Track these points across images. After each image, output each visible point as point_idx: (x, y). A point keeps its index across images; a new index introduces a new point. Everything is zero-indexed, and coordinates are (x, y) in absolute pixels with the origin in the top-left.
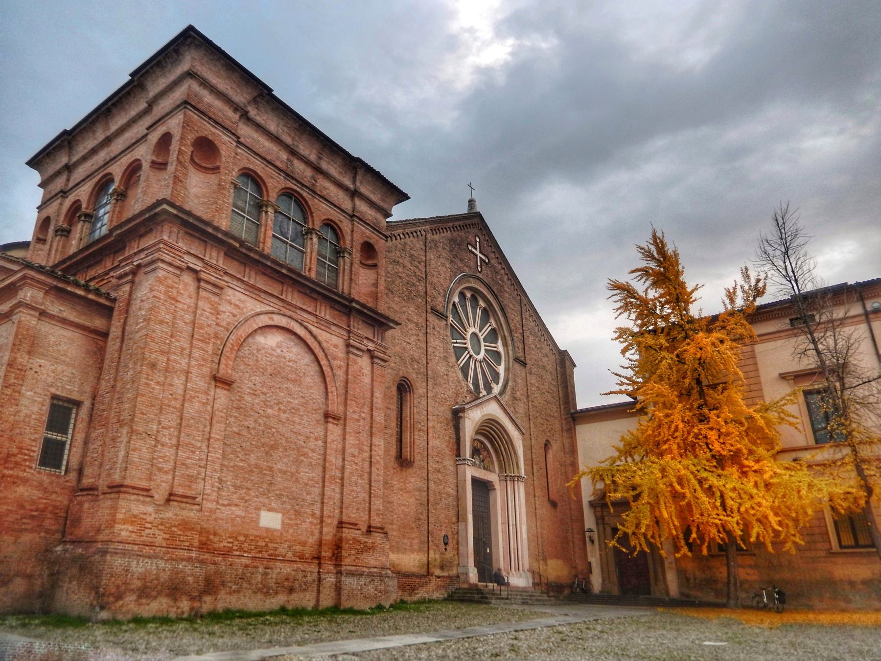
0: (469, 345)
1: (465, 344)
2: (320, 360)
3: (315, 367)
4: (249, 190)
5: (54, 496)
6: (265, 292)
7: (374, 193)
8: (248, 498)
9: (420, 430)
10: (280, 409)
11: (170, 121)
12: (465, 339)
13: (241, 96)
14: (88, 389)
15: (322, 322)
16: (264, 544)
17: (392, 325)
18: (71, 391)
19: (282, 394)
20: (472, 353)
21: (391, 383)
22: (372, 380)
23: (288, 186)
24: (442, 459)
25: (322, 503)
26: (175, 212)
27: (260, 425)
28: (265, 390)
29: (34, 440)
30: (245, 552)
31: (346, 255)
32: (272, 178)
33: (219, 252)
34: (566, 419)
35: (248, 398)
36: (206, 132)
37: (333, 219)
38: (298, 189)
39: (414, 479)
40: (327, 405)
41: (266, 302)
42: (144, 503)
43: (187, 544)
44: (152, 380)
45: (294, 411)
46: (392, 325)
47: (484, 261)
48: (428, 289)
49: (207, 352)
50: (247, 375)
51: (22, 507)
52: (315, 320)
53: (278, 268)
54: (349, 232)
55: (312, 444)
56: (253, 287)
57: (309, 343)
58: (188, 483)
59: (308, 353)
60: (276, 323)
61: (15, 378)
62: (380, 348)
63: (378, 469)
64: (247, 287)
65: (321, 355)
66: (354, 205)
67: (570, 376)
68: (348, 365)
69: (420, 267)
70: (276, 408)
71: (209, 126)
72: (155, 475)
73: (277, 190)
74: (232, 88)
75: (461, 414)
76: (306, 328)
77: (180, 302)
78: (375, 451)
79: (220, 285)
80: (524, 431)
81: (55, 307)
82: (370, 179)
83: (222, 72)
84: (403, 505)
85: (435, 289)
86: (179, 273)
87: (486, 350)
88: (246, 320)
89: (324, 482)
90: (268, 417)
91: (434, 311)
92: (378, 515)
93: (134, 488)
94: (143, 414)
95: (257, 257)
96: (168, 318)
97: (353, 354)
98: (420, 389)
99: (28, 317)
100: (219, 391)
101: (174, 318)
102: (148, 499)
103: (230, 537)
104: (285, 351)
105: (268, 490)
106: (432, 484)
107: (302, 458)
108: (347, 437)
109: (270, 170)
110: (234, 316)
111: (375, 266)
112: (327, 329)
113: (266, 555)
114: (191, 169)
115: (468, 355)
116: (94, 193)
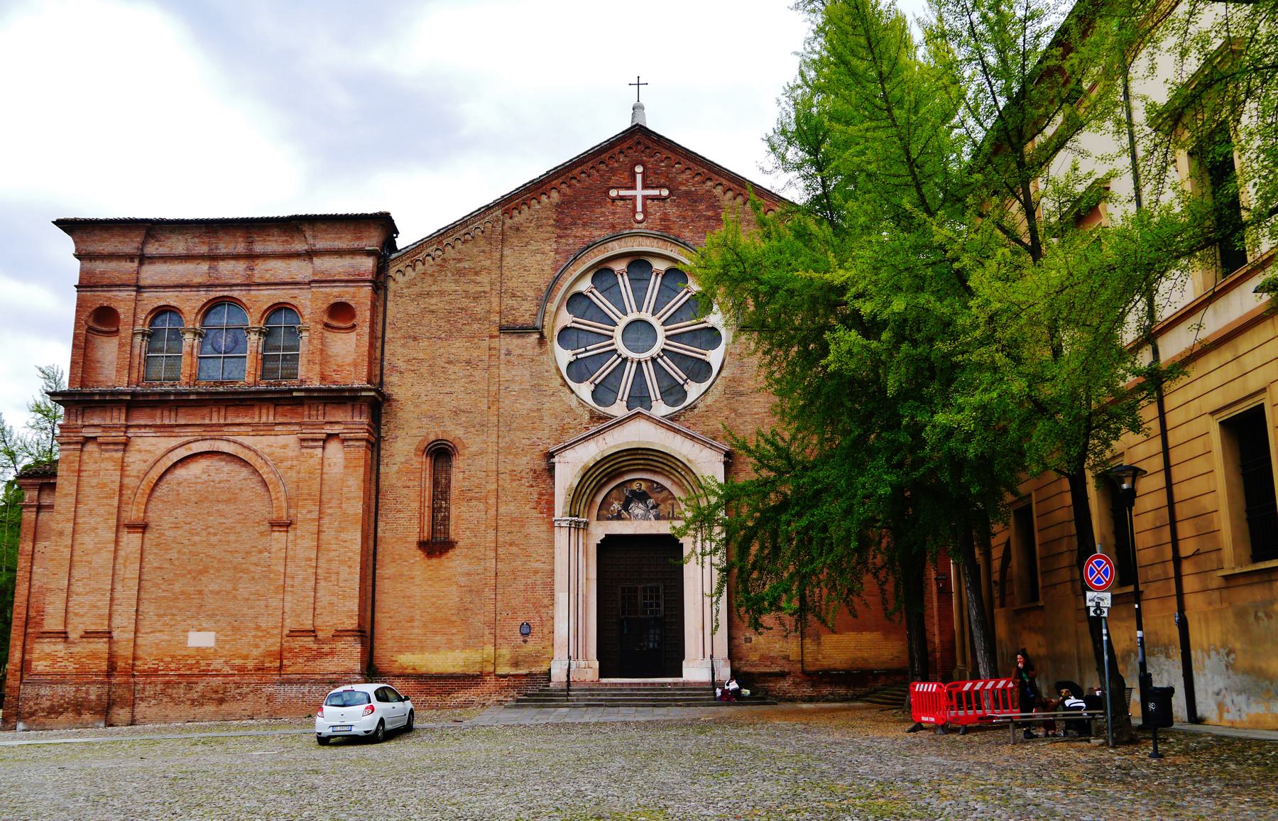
1: (613, 344)
3: (255, 478)
6: (177, 426)
7: (340, 238)
8: (173, 623)
13: (129, 245)
20: (625, 352)
24: (523, 526)
28: (189, 520)
32: (188, 300)
35: (170, 533)
37: (281, 300)
38: (226, 294)
39: (454, 563)
42: (55, 644)
47: (653, 198)
50: (166, 512)
52: (250, 429)
55: (254, 559)
56: (163, 426)
63: (350, 567)
65: (257, 463)
70: (204, 533)
75: (553, 460)
76: (235, 442)
82: (324, 227)
83: (105, 235)
84: (433, 597)
85: (514, 295)
86: (79, 447)
87: (667, 337)
90: (194, 544)
92: (351, 617)
97: (307, 447)
100: (130, 535)
105: (198, 614)
107: (241, 574)
109: (186, 293)
110: (145, 462)
113: (196, 671)
115: (620, 360)
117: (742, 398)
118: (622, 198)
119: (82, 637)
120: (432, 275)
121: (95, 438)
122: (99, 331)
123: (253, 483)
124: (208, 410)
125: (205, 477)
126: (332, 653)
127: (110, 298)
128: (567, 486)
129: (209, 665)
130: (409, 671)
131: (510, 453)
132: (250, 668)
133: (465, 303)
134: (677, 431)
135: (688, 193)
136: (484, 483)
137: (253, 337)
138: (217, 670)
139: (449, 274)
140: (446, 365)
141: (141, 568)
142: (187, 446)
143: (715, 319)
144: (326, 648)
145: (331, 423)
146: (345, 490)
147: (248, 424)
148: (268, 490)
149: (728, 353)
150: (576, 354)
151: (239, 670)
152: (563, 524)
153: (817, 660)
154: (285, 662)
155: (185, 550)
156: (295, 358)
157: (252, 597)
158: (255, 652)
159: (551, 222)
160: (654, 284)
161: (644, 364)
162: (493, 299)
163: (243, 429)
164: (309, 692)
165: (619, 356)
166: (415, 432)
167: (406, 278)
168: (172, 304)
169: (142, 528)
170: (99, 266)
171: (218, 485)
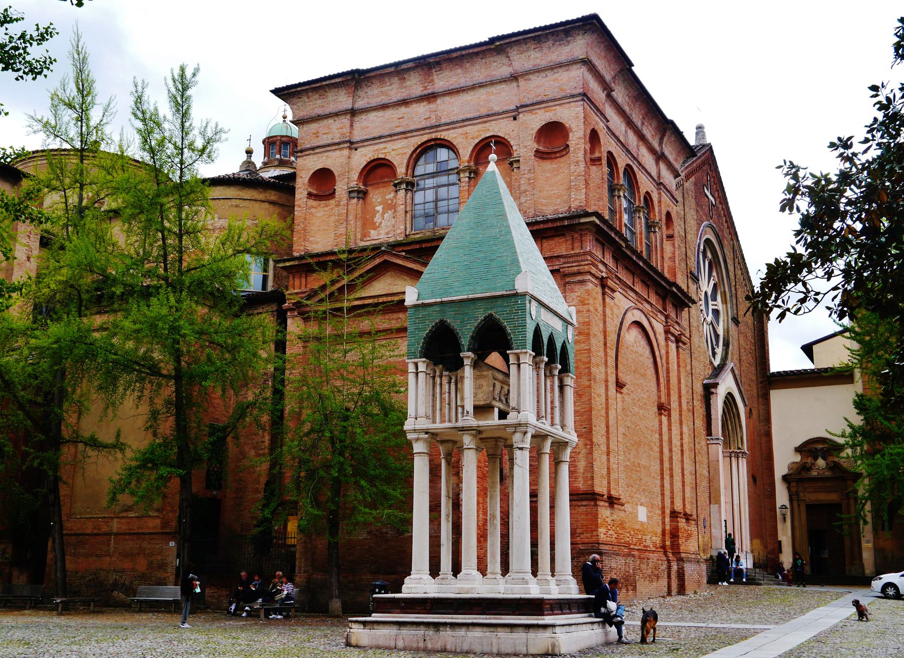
11: (557, 107)
34: (761, 382)
75: (713, 390)
80: (747, 403)
116: (414, 155)
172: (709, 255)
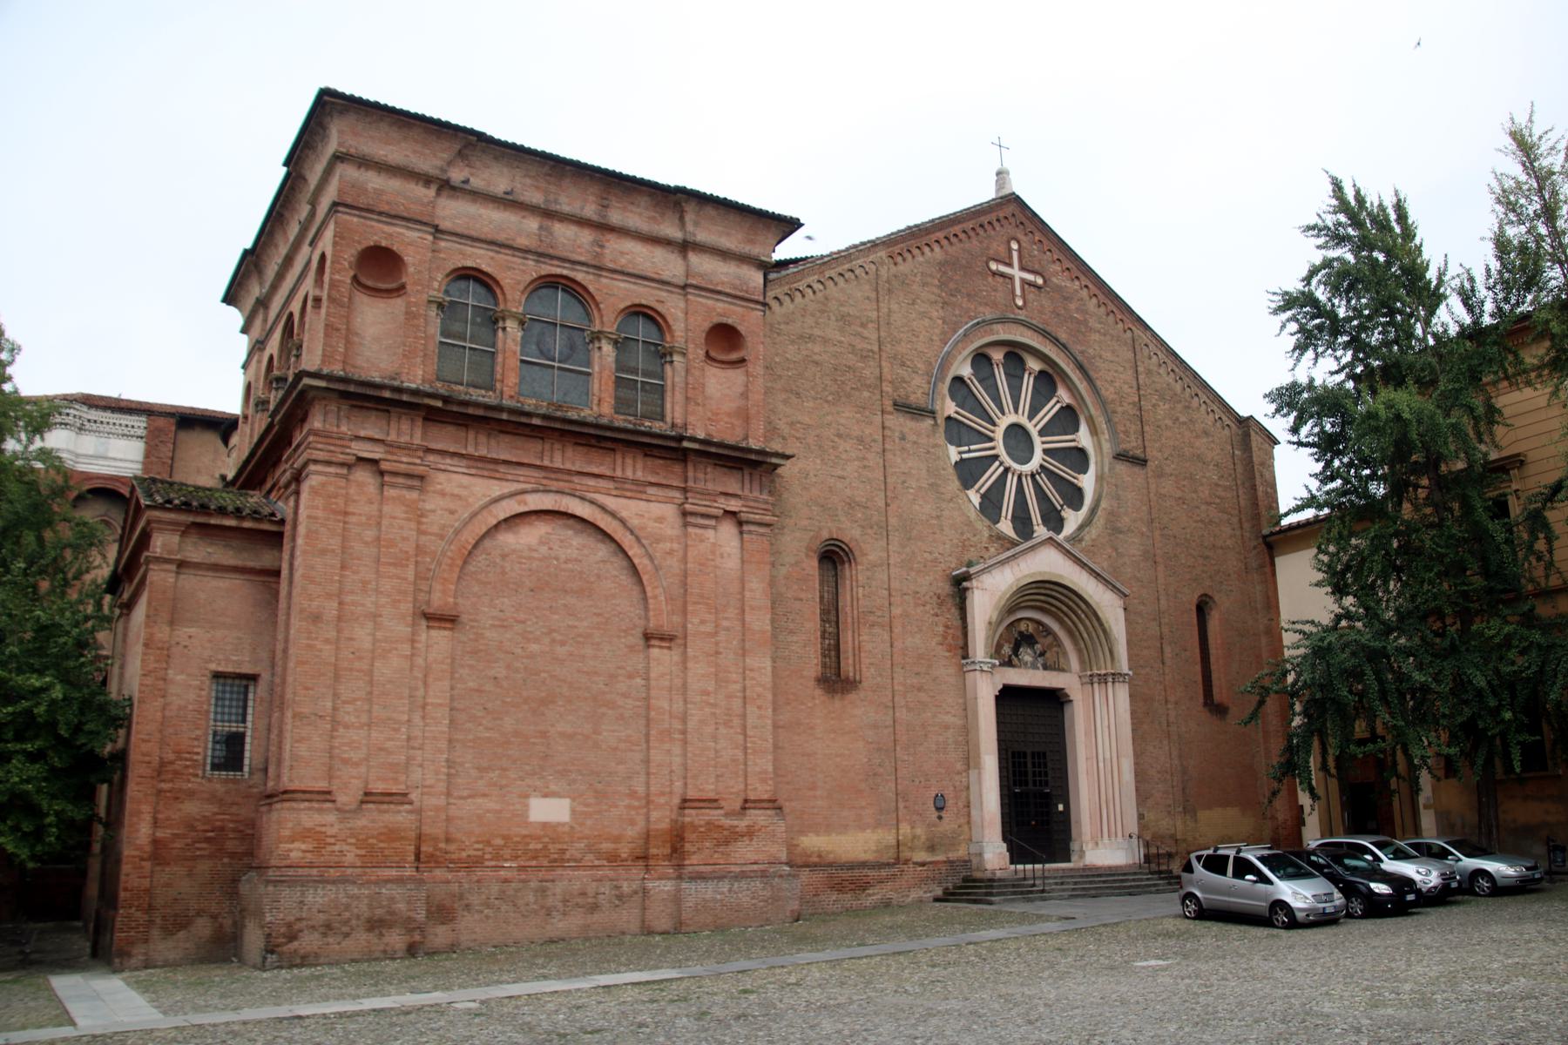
0: (1001, 450)
1: (993, 448)
2: (626, 549)
3: (619, 562)
4: (470, 302)
5: (234, 809)
7: (728, 234)
8: (504, 782)
9: (872, 626)
10: (553, 641)
12: (991, 439)
13: (429, 159)
14: (264, 655)
15: (627, 486)
16: (540, 846)
17: (774, 460)
18: (240, 663)
19: (556, 617)
21: (802, 555)
22: (743, 562)
23: (543, 273)
24: (930, 666)
25: (648, 774)
26: (322, 384)
27: (517, 671)
28: (522, 616)
29: (197, 739)
30: (506, 860)
31: (676, 358)
32: (509, 268)
33: (412, 420)
36: (376, 238)
37: (644, 302)
38: (565, 272)
39: (859, 710)
40: (647, 619)
41: (510, 477)
42: (320, 811)
43: (397, 859)
44: (316, 638)
45: (581, 639)
46: (774, 460)
47: (1031, 284)
48: (885, 370)
49: (406, 579)
51: (192, 828)
52: (611, 485)
53: (524, 420)
54: (681, 315)
55: (622, 687)
56: (482, 459)
57: (602, 525)
58: (391, 775)
59: (604, 542)
60: (533, 507)
61: (157, 661)
62: (752, 504)
63: (759, 708)
64: (471, 463)
65: (626, 540)
66: (688, 266)
67: (1262, 464)
68: (686, 546)
69: (866, 333)
70: (546, 640)
71: (381, 225)
72: (339, 770)
73: (521, 287)
74: (415, 152)
75: (965, 584)
76: (592, 502)
77: (354, 514)
78: (753, 679)
79: (416, 473)
80: (1127, 591)
81: (198, 551)
85: (903, 364)
86: (344, 471)
87: (1046, 451)
88: (474, 515)
89: (648, 741)
90: (532, 656)
91: (903, 407)
92: (764, 781)
93: (304, 792)
94: (307, 689)
95: (480, 412)
96: (335, 543)
97: (696, 526)
98: (870, 551)
99: (163, 575)
100: (434, 633)
101: (344, 539)
102: (328, 805)
103: (478, 842)
104: (556, 547)
106: (902, 714)
107: (603, 710)
108: (690, 665)
109: (504, 257)
110: (452, 512)
111: (743, 361)
112: (639, 495)
114: (362, 301)
115: (1002, 469)
117: (1121, 536)
118: (1002, 275)
119: (362, 802)
120: (813, 315)
121: (375, 462)
122: (359, 283)
123: (616, 567)
124: (539, 447)
125: (544, 550)
126: (750, 833)
127: (391, 235)
128: (987, 618)
129: (563, 851)
130: (815, 859)
131: (912, 569)
132: (624, 856)
133: (851, 360)
134: (1083, 565)
135: (1059, 289)
136: (887, 604)
137: (607, 348)
138: (575, 861)
139: (833, 318)
140: (836, 439)
141: (452, 688)
142: (519, 497)
143: (1084, 438)
144: (742, 824)
145: (726, 494)
146: (747, 594)
147: (612, 478)
148: (640, 582)
149: (1100, 478)
150: (960, 453)
151: (609, 861)
152: (985, 668)
153: (1195, 839)
154: (688, 847)
155: (519, 665)
156: (661, 390)
157: (622, 746)
158: (631, 832)
159: (936, 282)
160: (1028, 383)
161: (1024, 479)
162: (884, 364)
163: (602, 483)
164: (730, 891)
165: (1001, 464)
166: (806, 522)
167: (784, 310)
168: (484, 267)
169: (445, 619)
170: (374, 181)
171: (563, 566)
172: (1034, 365)
